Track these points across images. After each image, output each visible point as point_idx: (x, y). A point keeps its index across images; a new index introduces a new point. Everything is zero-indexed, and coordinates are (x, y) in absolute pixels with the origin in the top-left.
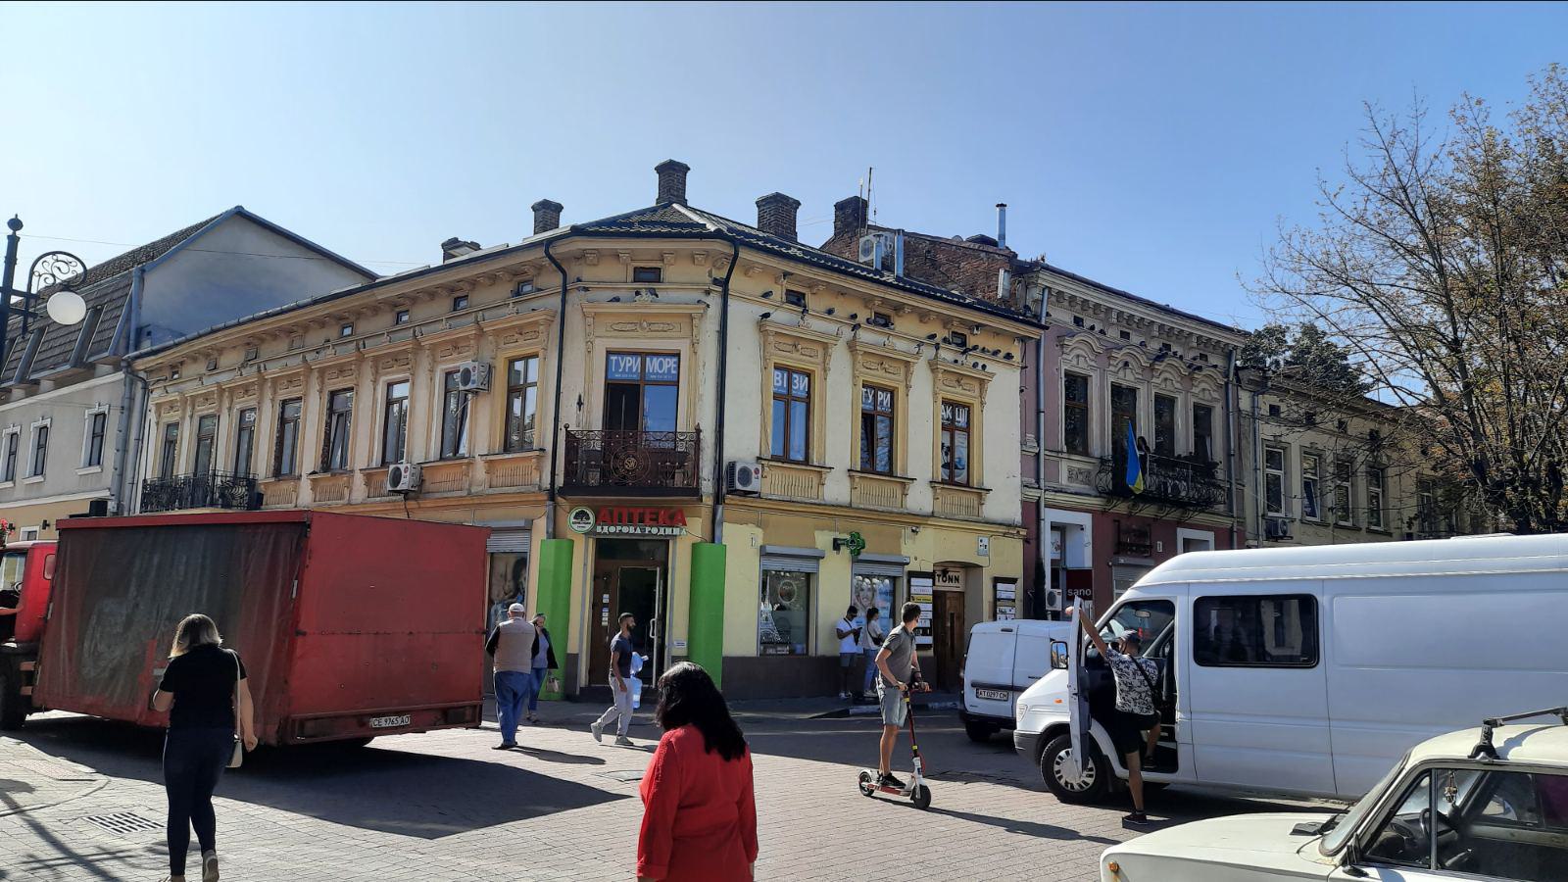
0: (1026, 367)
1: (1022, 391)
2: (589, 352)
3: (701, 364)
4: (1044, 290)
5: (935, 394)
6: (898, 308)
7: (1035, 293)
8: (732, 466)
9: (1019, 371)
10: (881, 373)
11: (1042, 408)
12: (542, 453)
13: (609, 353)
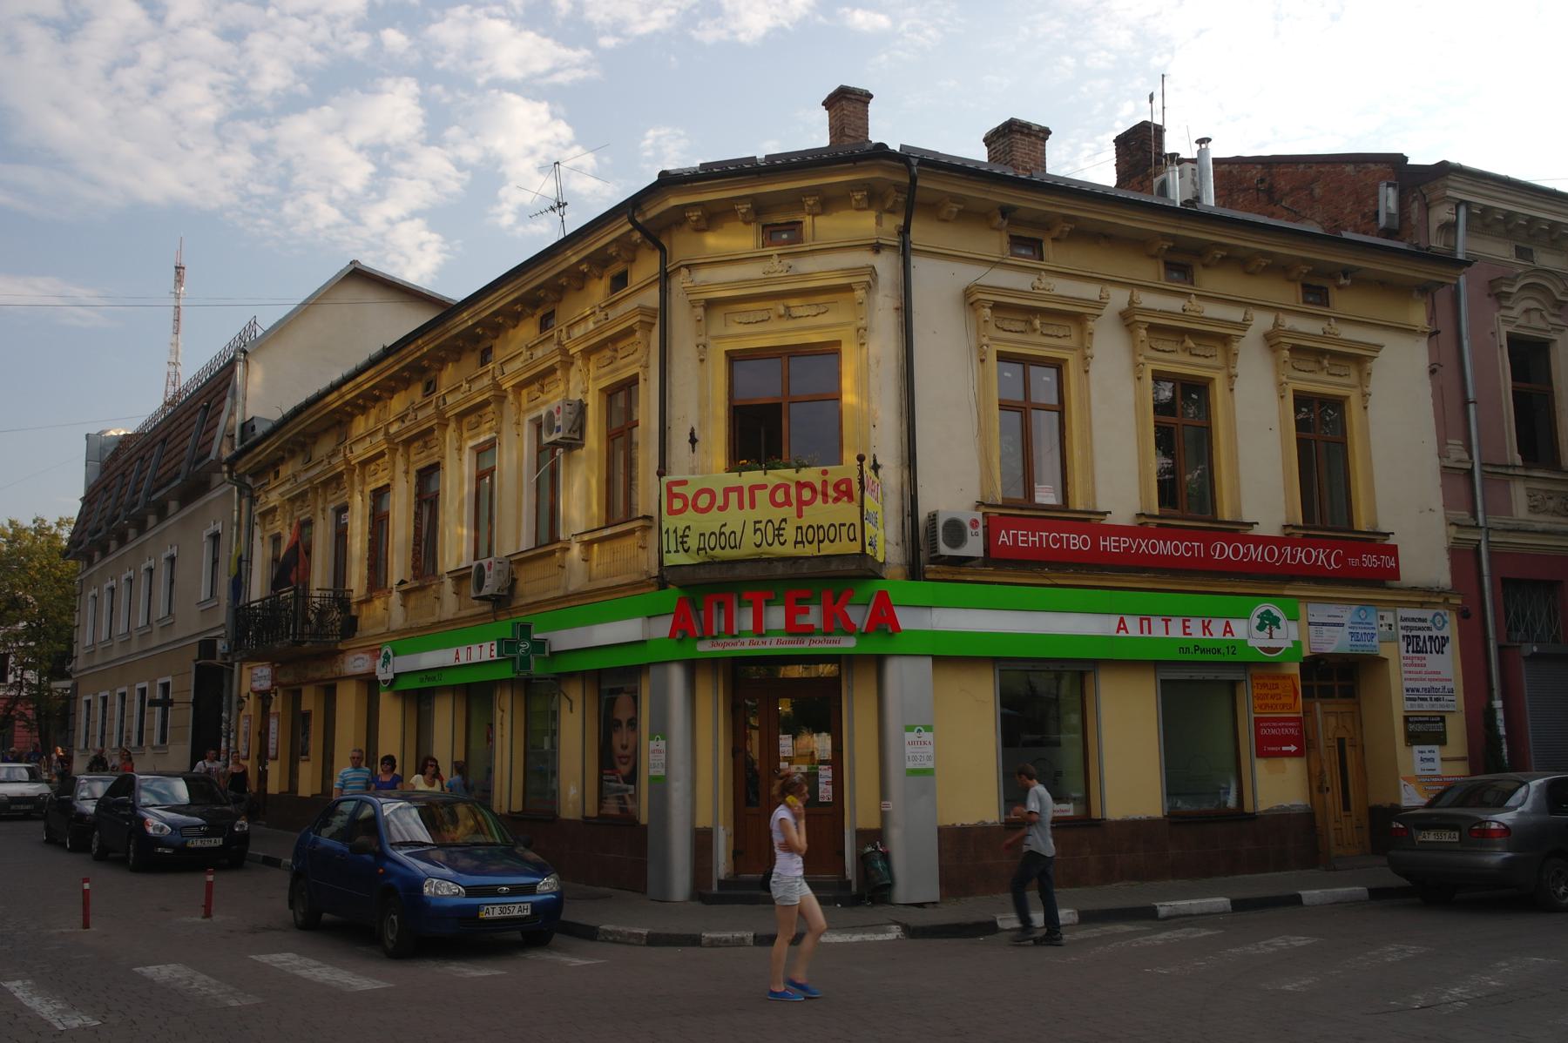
0: (1437, 332)
1: (1433, 372)
2: (702, 361)
4: (1457, 207)
5: (1281, 385)
7: (1442, 213)
8: (933, 518)
9: (1425, 339)
10: (1185, 357)
11: (1471, 395)
12: (647, 523)
13: (733, 357)
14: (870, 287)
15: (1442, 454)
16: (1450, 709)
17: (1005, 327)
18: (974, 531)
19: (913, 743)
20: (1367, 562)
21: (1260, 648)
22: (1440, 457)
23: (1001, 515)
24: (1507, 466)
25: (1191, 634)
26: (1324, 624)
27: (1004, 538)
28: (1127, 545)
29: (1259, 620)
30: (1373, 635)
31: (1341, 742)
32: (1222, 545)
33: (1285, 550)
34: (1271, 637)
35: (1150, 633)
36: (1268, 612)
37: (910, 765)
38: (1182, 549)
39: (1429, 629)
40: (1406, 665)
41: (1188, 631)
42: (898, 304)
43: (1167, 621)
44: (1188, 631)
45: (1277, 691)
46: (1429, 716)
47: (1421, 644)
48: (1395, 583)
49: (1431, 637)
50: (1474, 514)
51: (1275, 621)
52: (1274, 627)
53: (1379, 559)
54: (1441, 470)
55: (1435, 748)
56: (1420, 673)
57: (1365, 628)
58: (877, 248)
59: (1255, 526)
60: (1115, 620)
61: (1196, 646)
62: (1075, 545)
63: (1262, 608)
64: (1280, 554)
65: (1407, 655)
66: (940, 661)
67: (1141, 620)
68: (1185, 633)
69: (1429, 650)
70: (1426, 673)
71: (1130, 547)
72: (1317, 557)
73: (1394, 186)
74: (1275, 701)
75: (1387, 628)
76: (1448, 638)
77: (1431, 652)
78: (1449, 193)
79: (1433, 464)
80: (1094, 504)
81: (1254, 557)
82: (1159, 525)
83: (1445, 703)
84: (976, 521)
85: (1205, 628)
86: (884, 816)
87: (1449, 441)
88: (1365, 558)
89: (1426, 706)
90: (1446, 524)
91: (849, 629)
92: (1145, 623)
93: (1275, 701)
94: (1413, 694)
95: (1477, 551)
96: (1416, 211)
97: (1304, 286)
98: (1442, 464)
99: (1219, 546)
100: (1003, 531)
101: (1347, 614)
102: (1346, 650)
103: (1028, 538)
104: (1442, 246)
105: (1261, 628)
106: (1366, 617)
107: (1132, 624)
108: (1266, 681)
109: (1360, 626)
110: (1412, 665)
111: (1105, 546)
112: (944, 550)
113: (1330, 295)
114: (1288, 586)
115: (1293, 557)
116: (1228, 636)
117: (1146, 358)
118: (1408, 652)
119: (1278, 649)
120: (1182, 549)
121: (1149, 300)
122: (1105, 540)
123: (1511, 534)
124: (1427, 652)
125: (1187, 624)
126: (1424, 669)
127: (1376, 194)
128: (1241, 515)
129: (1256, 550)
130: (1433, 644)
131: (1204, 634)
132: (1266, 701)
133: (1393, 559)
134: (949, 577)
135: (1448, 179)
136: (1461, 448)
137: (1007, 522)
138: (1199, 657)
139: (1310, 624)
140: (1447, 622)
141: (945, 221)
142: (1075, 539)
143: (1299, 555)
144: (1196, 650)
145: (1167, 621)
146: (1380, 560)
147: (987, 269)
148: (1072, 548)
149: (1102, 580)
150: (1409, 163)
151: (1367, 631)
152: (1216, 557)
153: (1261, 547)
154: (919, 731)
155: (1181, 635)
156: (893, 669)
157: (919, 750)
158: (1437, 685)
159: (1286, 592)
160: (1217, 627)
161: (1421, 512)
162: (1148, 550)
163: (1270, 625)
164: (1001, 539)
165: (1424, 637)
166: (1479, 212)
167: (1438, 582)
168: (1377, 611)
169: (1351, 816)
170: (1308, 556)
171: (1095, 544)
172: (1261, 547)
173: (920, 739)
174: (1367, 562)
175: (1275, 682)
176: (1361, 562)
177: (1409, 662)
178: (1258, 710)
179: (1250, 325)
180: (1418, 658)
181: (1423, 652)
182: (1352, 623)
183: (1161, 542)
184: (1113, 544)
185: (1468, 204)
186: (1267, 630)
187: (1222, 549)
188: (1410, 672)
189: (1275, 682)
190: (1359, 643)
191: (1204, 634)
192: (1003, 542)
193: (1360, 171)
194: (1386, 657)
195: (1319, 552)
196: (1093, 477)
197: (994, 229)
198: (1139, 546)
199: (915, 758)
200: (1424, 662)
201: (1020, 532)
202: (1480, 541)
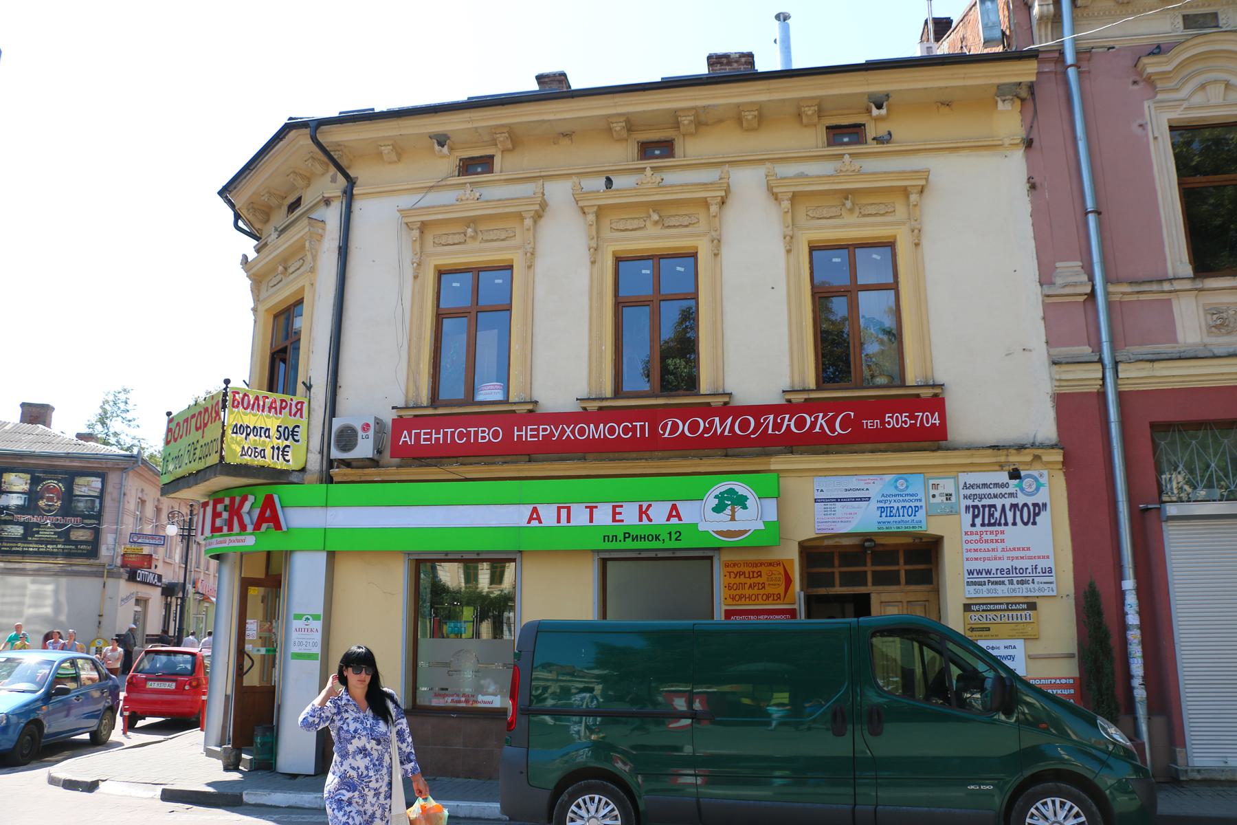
6: (674, 119)
10: (652, 230)
11: (1090, 205)
15: (1045, 279)
16: (1046, 593)
18: (364, 434)
19: (300, 630)
21: (717, 532)
22: (1041, 285)
23: (416, 416)
24: (1160, 281)
25: (622, 521)
26: (837, 500)
27: (405, 437)
29: (716, 501)
30: (917, 508)
32: (673, 422)
33: (765, 420)
34: (733, 519)
35: (569, 521)
36: (731, 491)
38: (619, 430)
39: (1011, 495)
40: (967, 542)
41: (618, 517)
43: (591, 509)
44: (618, 517)
45: (759, 580)
46: (1008, 604)
47: (997, 515)
48: (943, 443)
49: (1014, 506)
52: (738, 508)
54: (1043, 301)
55: (1020, 644)
56: (993, 550)
57: (904, 501)
60: (527, 511)
61: (625, 534)
62: (483, 438)
63: (723, 485)
64: (758, 425)
65: (974, 529)
67: (559, 509)
68: (614, 520)
69: (1010, 520)
70: (1003, 550)
71: (552, 433)
72: (814, 424)
74: (755, 591)
75: (944, 498)
76: (1045, 505)
77: (1014, 524)
81: (719, 431)
83: (1036, 586)
84: (368, 425)
85: (643, 513)
87: (1058, 264)
88: (889, 417)
89: (1002, 591)
90: (1049, 364)
92: (564, 512)
93: (755, 591)
94: (976, 577)
95: (1102, 395)
98: (1044, 293)
99: (670, 423)
100: (405, 432)
101: (876, 487)
102: (873, 528)
103: (432, 436)
105: (718, 509)
106: (907, 487)
107: (548, 515)
108: (742, 569)
109: (897, 498)
110: (980, 541)
111: (520, 437)
118: (973, 525)
119: (745, 532)
122: (520, 430)
124: (1006, 524)
125: (618, 510)
126: (1000, 546)
130: (1018, 513)
131: (641, 520)
132: (743, 592)
136: (1080, 269)
137: (420, 421)
138: (629, 544)
139: (816, 501)
140: (1043, 485)
142: (483, 432)
143: (786, 423)
144: (625, 538)
145: (591, 509)
147: (420, 196)
148: (480, 441)
151: (907, 505)
152: (666, 436)
153: (729, 420)
154: (308, 619)
157: (304, 636)
158: (1019, 564)
159: (773, 467)
160: (659, 513)
162: (574, 435)
163: (733, 504)
164: (403, 439)
165: (1004, 506)
167: (1035, 437)
171: (508, 434)
172: (729, 420)
174: (893, 422)
175: (756, 570)
176: (883, 422)
177: (977, 537)
178: (730, 601)
180: (992, 533)
181: (1000, 524)
182: (883, 495)
183: (592, 426)
184: (529, 433)
186: (728, 511)
187: (675, 427)
188: (976, 550)
189: (756, 570)
190: (889, 519)
191: (641, 520)
194: (942, 535)
195: (817, 418)
198: (563, 431)
199: (300, 644)
200: (1000, 537)
201: (423, 431)
202: (1103, 379)
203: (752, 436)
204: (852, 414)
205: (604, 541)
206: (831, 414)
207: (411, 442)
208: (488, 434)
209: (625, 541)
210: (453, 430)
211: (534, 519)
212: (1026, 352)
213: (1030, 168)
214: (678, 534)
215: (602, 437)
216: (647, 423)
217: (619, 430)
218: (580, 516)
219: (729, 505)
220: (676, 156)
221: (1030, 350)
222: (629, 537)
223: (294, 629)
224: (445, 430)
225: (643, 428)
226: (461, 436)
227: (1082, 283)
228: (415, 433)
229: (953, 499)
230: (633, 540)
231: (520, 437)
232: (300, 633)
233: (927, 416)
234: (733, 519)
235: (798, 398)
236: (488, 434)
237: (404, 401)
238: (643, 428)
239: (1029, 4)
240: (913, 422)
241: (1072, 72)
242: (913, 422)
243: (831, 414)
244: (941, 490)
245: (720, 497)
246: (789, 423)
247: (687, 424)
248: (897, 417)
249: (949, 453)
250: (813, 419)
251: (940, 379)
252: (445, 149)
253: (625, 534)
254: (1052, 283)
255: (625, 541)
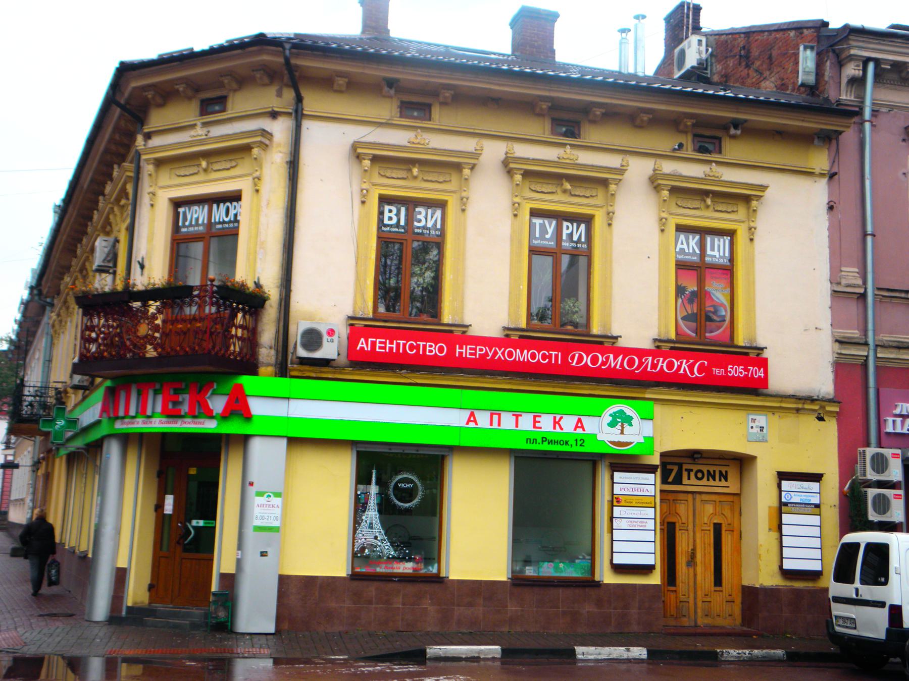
3: (264, 203)
7: (852, 70)
9: (824, 181)
11: (869, 229)
14: (265, 147)
17: (388, 175)
18: (330, 338)
19: (262, 506)
20: (733, 372)
21: (610, 442)
23: (366, 326)
25: (540, 428)
27: (362, 344)
28: (483, 352)
29: (611, 418)
31: (718, 528)
33: (646, 360)
34: (622, 433)
35: (499, 425)
36: (621, 412)
37: (257, 523)
41: (538, 425)
42: (288, 159)
43: (517, 416)
44: (538, 425)
48: (765, 391)
50: (865, 332)
51: (628, 420)
53: (746, 370)
54: (831, 294)
58: (274, 115)
59: (619, 338)
61: (543, 438)
62: (431, 351)
63: (617, 406)
64: (641, 364)
66: (294, 442)
67: (492, 415)
68: (535, 427)
71: (486, 354)
72: (679, 367)
73: (812, 48)
75: (759, 430)
78: (853, 52)
79: (824, 289)
80: (462, 318)
81: (613, 365)
82: (521, 337)
85: (556, 423)
86: (239, 562)
87: (843, 269)
88: (731, 368)
91: (210, 415)
92: (495, 417)
95: (865, 365)
96: (828, 68)
97: (695, 136)
98: (833, 289)
99: (577, 355)
100: (362, 340)
104: (852, 98)
105: (612, 425)
107: (483, 419)
111: (461, 353)
112: (302, 353)
113: (723, 144)
114: (648, 390)
115: (654, 366)
116: (579, 430)
117: (525, 199)
119: (631, 443)
120: (539, 356)
121: (522, 150)
122: (461, 348)
123: (902, 351)
125: (538, 419)
127: (796, 56)
128: (610, 329)
129: (615, 359)
131: (555, 428)
133: (762, 369)
134: (314, 375)
135: (850, 39)
136: (856, 275)
138: (546, 447)
141: (340, 92)
142: (431, 346)
143: (660, 364)
144: (543, 441)
145: (517, 416)
146: (748, 371)
148: (428, 353)
149: (458, 380)
150: (831, 26)
152: (574, 364)
153: (620, 358)
155: (530, 427)
156: (257, 447)
159: (647, 396)
160: (568, 424)
161: (805, 330)
164: (360, 345)
166: (889, 67)
167: (819, 391)
168: (748, 414)
169: (722, 591)
170: (670, 365)
171: (451, 350)
172: (620, 358)
173: (269, 503)
174: (733, 372)
176: (726, 371)
179: (626, 170)
184: (468, 351)
185: (877, 61)
187: (580, 359)
191: (555, 428)
192: (362, 348)
193: (798, 36)
194: (755, 455)
195: (681, 363)
196: (463, 297)
197: (384, 97)
198: (496, 353)
199: (262, 518)
201: (378, 340)
202: (867, 357)
203: (636, 372)
204: (706, 363)
205: (527, 443)
206: (692, 361)
207: (367, 347)
208: (435, 349)
209: (542, 443)
210: (405, 342)
211: (472, 421)
212: (817, 330)
213: (830, 194)
214: (582, 441)
215: (526, 360)
216: (560, 353)
217: (539, 356)
218: (508, 421)
219: (619, 422)
220: (582, 137)
221: (820, 329)
222: (546, 441)
223: (256, 505)
224: (398, 341)
225: (556, 356)
226: (412, 347)
227: (859, 286)
228: (372, 341)
229: (765, 430)
230: (549, 443)
231: (461, 353)
232: (262, 508)
233: (756, 370)
234: (622, 433)
235: (666, 347)
236: (435, 349)
237: (352, 310)
238: (556, 356)
239: (842, 63)
240: (746, 373)
241: (867, 125)
242: (746, 373)
243: (692, 361)
244: (757, 424)
245: (614, 416)
246: (662, 364)
247: (590, 356)
248: (736, 368)
249: (767, 398)
250: (679, 364)
251: (761, 343)
252: (392, 92)
253: (543, 438)
254: (839, 284)
255: (542, 443)
